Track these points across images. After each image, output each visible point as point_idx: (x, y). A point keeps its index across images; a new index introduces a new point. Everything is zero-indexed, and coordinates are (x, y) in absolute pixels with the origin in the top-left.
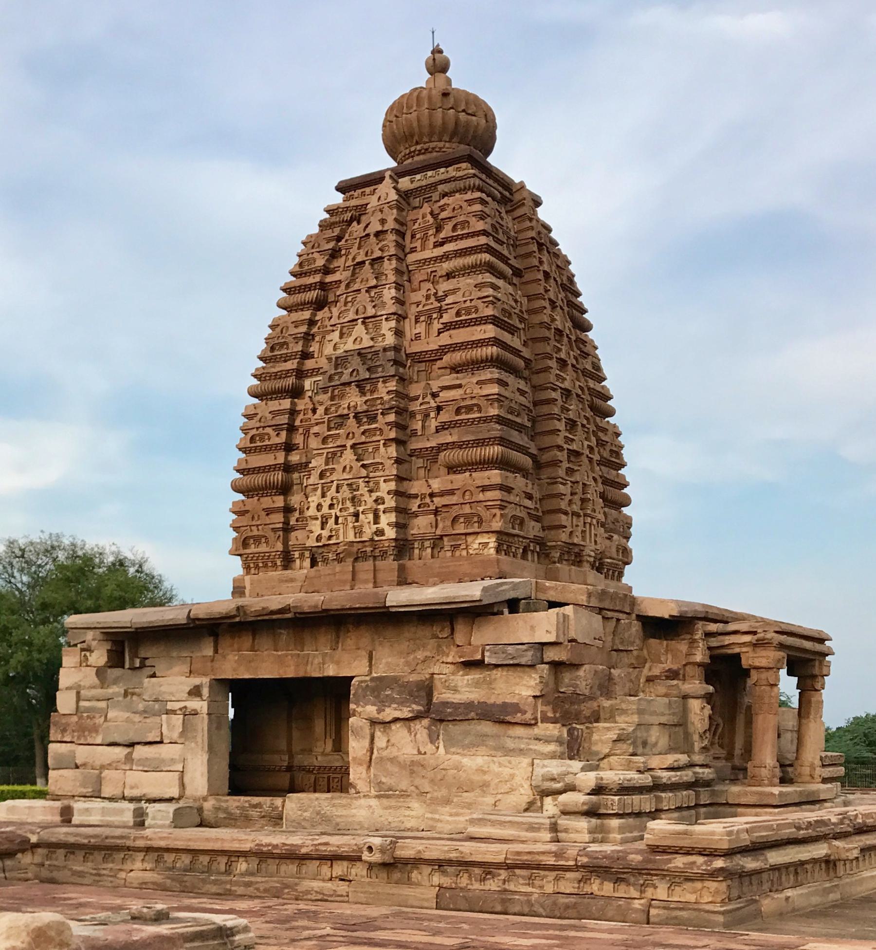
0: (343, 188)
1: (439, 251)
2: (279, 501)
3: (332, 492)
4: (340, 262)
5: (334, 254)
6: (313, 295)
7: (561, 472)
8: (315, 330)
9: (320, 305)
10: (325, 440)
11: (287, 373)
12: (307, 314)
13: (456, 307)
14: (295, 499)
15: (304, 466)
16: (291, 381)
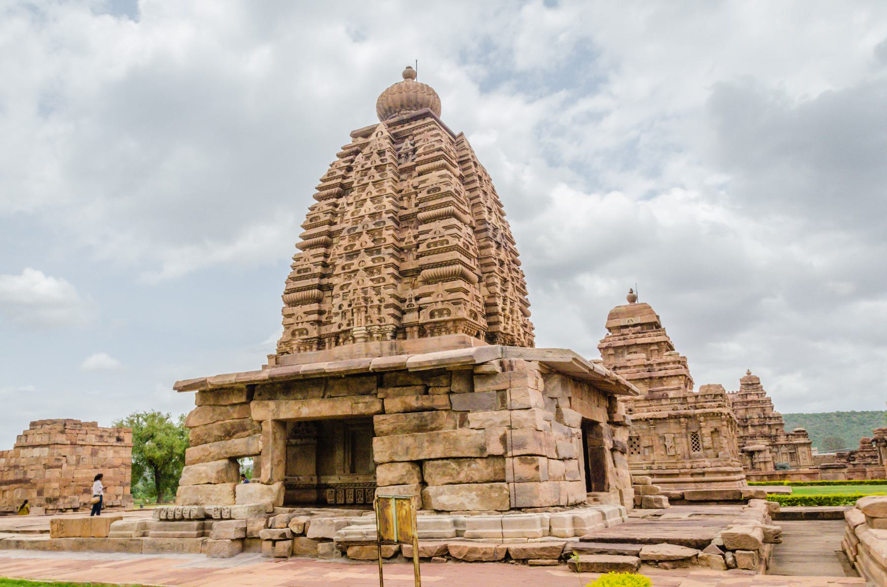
0: (355, 135)
1: (414, 163)
2: (315, 307)
3: (351, 296)
4: (352, 174)
5: (349, 169)
6: (337, 189)
7: (498, 290)
8: (338, 209)
9: (339, 196)
10: (343, 268)
11: (320, 234)
12: (334, 200)
13: (427, 189)
14: (325, 307)
15: (330, 287)
16: (323, 238)
